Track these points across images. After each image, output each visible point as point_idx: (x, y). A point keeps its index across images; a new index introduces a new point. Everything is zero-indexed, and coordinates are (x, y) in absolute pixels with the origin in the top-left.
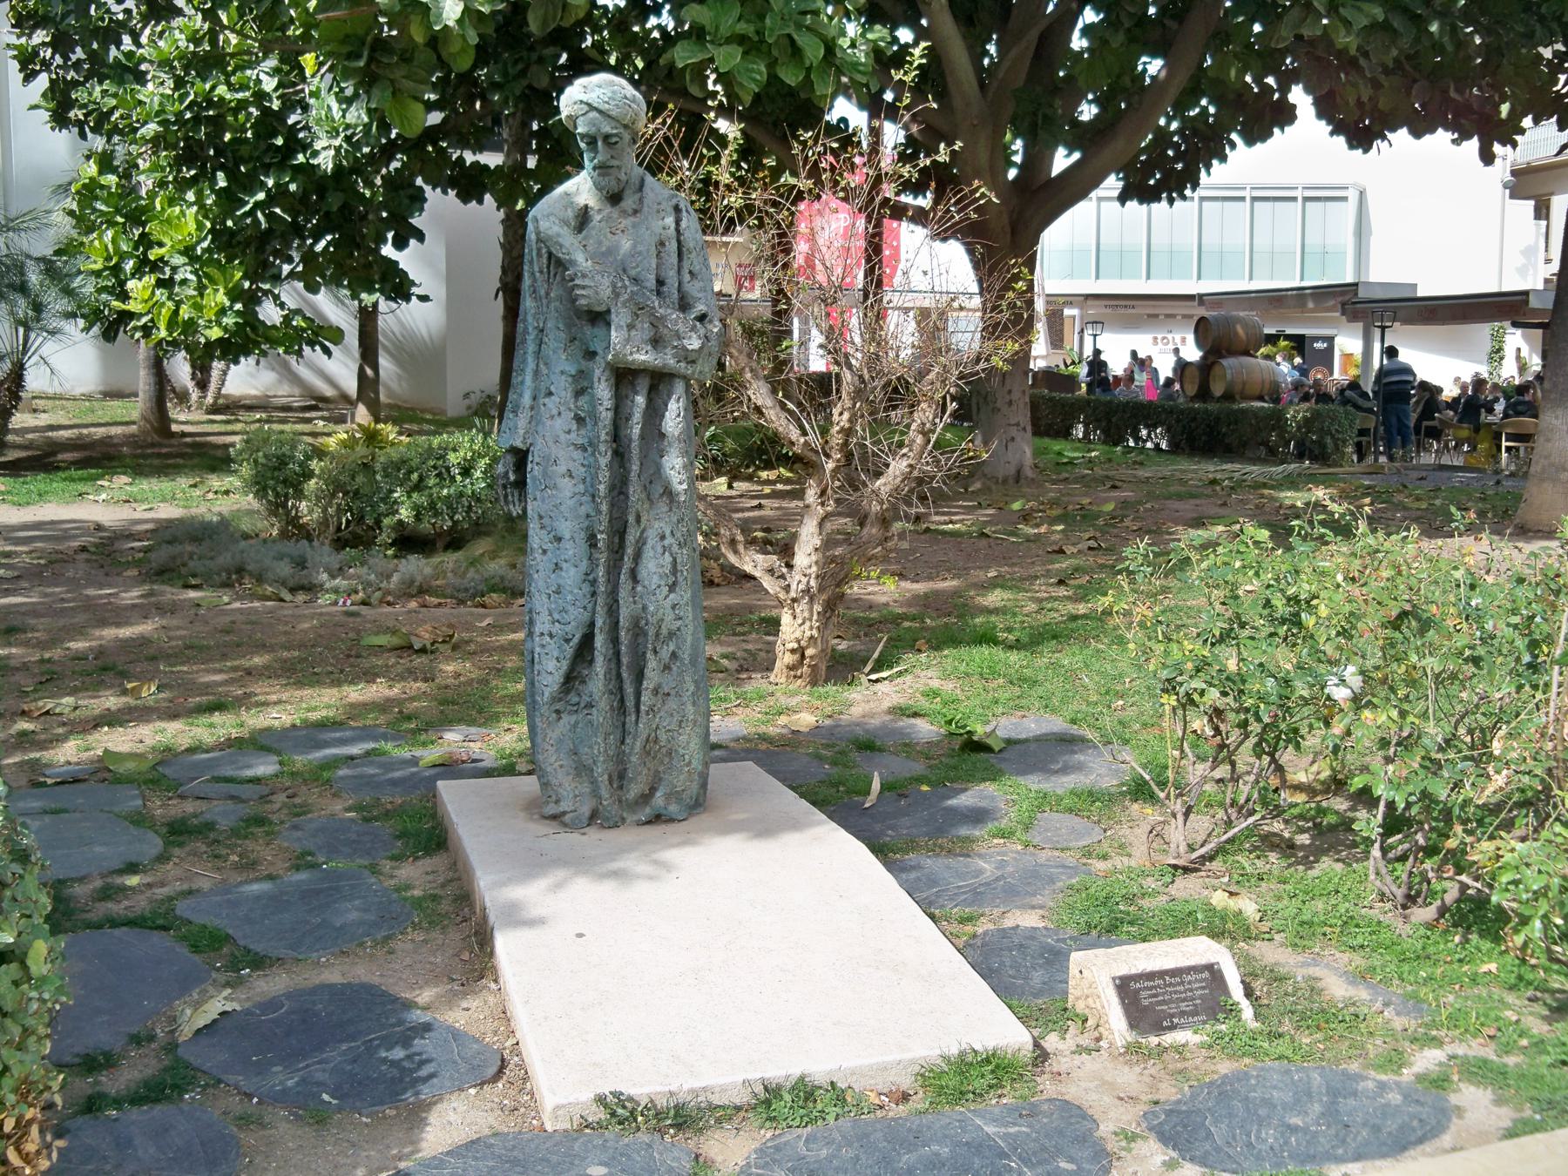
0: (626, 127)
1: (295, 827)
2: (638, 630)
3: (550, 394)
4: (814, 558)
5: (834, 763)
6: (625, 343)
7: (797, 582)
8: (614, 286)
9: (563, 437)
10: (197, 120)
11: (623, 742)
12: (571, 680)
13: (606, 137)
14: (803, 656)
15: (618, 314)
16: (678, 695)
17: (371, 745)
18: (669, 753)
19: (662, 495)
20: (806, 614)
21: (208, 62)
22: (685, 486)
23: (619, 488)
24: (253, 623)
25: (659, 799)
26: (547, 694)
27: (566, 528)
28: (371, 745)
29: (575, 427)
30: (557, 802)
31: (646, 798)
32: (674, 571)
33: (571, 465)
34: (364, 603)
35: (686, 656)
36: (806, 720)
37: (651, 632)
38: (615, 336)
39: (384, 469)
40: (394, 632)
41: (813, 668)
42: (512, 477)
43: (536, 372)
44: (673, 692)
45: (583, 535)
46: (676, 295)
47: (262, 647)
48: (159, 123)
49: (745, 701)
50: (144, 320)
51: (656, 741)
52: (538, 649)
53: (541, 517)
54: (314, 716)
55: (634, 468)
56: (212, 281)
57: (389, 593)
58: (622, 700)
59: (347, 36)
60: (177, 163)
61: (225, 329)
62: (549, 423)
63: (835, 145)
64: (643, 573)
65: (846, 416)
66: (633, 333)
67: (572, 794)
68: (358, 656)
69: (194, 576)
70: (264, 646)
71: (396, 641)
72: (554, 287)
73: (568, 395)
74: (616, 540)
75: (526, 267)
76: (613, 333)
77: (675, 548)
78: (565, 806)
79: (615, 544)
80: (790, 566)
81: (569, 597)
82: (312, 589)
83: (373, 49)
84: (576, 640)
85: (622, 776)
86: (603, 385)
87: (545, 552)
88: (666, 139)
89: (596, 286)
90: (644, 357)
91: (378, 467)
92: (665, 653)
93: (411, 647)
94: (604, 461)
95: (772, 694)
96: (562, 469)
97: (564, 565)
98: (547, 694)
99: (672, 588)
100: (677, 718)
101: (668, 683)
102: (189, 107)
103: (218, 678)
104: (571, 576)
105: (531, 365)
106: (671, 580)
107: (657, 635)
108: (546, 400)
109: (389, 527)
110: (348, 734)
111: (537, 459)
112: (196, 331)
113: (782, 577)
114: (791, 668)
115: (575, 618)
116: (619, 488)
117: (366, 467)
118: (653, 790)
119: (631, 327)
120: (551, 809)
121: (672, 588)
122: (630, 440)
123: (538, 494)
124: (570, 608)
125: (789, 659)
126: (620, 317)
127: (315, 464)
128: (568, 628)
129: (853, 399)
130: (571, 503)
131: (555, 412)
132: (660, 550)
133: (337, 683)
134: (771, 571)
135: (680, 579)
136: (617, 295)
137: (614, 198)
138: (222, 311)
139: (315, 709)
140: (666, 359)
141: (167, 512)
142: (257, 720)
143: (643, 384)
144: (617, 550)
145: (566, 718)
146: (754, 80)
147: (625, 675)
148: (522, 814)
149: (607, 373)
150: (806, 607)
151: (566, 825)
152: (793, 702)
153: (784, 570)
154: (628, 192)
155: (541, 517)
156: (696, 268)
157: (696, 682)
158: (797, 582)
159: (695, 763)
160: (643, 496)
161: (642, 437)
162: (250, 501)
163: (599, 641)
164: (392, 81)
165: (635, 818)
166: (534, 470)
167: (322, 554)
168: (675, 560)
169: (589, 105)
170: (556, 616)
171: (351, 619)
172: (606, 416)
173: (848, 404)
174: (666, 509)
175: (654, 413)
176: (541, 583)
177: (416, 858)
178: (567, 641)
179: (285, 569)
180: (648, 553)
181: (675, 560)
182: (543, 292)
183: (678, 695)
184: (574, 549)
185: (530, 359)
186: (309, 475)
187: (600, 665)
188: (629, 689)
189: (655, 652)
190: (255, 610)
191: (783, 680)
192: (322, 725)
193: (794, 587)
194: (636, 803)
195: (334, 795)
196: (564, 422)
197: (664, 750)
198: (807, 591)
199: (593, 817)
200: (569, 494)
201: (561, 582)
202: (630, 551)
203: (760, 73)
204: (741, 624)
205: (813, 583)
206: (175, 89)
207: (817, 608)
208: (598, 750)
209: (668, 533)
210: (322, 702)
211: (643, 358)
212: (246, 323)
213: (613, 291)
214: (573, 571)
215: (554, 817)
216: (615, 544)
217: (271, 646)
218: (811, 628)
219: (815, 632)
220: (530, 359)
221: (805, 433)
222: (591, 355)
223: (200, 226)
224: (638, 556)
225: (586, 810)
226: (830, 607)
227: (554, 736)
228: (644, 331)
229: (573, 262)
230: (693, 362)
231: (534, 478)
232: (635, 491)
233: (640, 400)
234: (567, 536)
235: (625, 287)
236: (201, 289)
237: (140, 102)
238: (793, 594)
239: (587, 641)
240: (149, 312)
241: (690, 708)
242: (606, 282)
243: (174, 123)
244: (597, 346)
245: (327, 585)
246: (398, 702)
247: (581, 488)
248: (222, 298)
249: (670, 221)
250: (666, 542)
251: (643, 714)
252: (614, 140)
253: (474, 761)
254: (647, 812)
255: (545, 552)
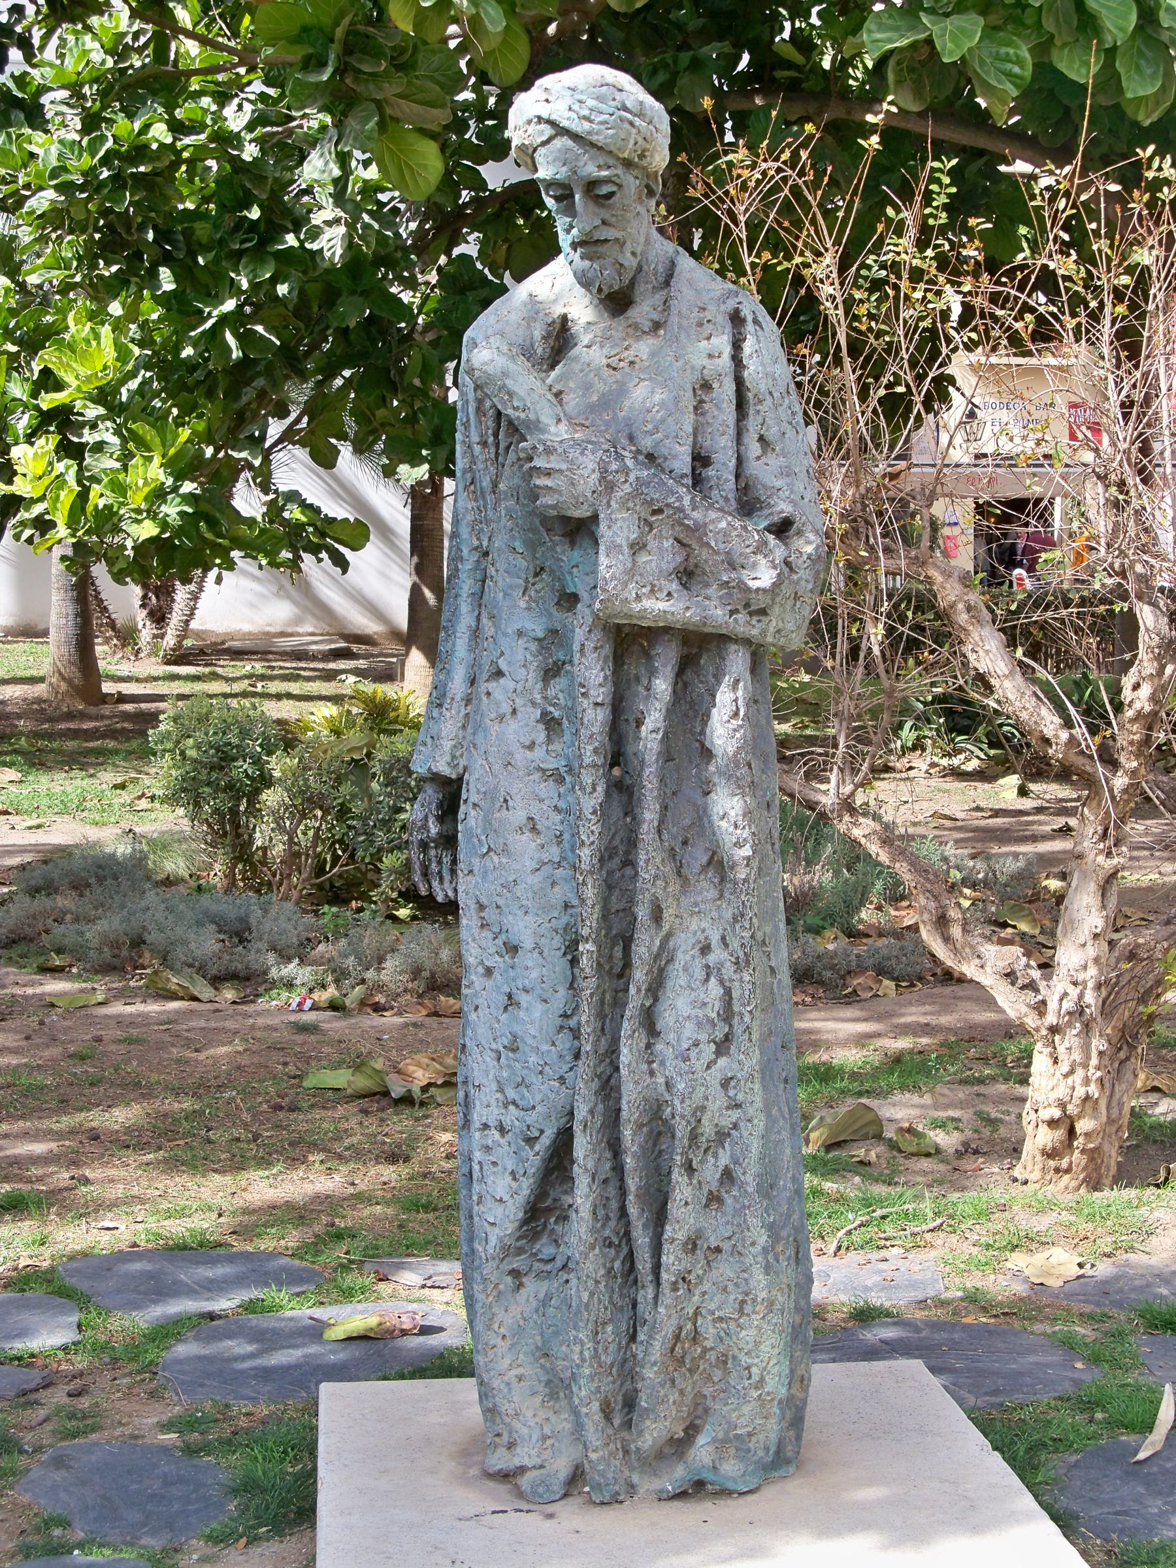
0: (628, 164)
1: (59, 1462)
2: (657, 1125)
3: (499, 674)
4: (1091, 952)
5: (1095, 1360)
6: (629, 577)
7: (1058, 993)
8: (604, 471)
9: (521, 757)
10: (118, 180)
11: (633, 1338)
12: (542, 1213)
13: (591, 186)
14: (1072, 1132)
15: (612, 522)
16: (736, 1252)
17: (255, 1293)
18: (723, 1361)
19: (705, 868)
20: (1077, 1056)
21: (125, 89)
22: (747, 851)
23: (619, 857)
24: (130, 1041)
25: (702, 1451)
26: (493, 1241)
27: (524, 929)
28: (255, 1293)
29: (541, 736)
30: (511, 1446)
31: (680, 1445)
32: (727, 1014)
33: (535, 810)
34: (334, 1006)
35: (750, 1179)
36: (1060, 1263)
37: (681, 1130)
38: (608, 565)
39: (386, 773)
40: (359, 1064)
41: (1093, 1155)
42: (434, 829)
43: (476, 633)
44: (726, 1246)
45: (557, 941)
46: (731, 485)
47: (134, 1088)
48: (57, 188)
49: (949, 1222)
50: (37, 509)
51: (696, 1337)
52: (478, 1155)
53: (481, 907)
54: (177, 1228)
55: (648, 815)
56: (142, 443)
57: (380, 987)
58: (631, 1257)
59: (305, 29)
60: (88, 259)
61: (164, 525)
62: (495, 728)
63: (1114, 188)
64: (666, 1020)
65: (1146, 690)
66: (643, 558)
67: (542, 1439)
68: (293, 1109)
69: (59, 951)
70: (138, 1085)
71: (362, 1082)
72: (507, 471)
73: (531, 676)
74: (618, 952)
75: (458, 436)
76: (603, 560)
77: (729, 971)
78: (525, 1455)
79: (613, 965)
80: (1046, 966)
81: (533, 1059)
82: (250, 982)
83: (348, 50)
84: (546, 1140)
85: (630, 1403)
86: (591, 657)
87: (489, 972)
88: (796, 191)
89: (572, 467)
90: (662, 605)
91: (377, 769)
92: (710, 1172)
93: (386, 1093)
94: (590, 803)
95: (1003, 1208)
96: (518, 816)
97: (523, 998)
98: (493, 1241)
99: (723, 1046)
100: (734, 1295)
101: (716, 1229)
102: (105, 161)
103: (39, 1148)
104: (536, 1019)
105: (466, 620)
106: (720, 1032)
107: (694, 1136)
108: (492, 686)
109: (392, 871)
110: (221, 1271)
111: (474, 798)
112: (117, 530)
113: (1031, 986)
114: (1050, 1154)
115: (544, 1094)
116: (619, 857)
117: (360, 767)
118: (692, 1430)
119: (637, 547)
120: (500, 1460)
121: (723, 1046)
122: (642, 763)
123: (476, 861)
124: (533, 1079)
125: (1045, 1137)
126: (617, 528)
127: (278, 765)
128: (531, 1118)
129: (1158, 658)
130: (535, 880)
131: (506, 708)
132: (699, 974)
133: (237, 1165)
134: (1010, 976)
135: (738, 1029)
136: (610, 487)
137: (616, 302)
138: (159, 494)
139: (182, 1213)
140: (710, 610)
141: (64, 832)
142: (72, 1237)
143: (666, 658)
144: (617, 972)
145: (532, 1286)
146: (1009, 75)
147: (633, 1210)
148: (450, 1465)
149: (597, 635)
150: (1076, 1042)
151: (521, 1495)
152: (1042, 1223)
153: (1036, 974)
154: (641, 288)
155: (481, 907)
156: (772, 433)
157: (771, 1228)
158: (1058, 993)
159: (771, 1384)
160: (668, 869)
161: (667, 756)
162: (172, 820)
163: (581, 1146)
164: (379, 105)
165: (656, 1484)
166: (470, 818)
167: (281, 916)
168: (728, 992)
169: (552, 123)
170: (511, 1094)
171: (299, 1038)
172: (596, 719)
173: (1149, 668)
174: (712, 894)
175: (689, 711)
176: (481, 1030)
177: (253, 1540)
178: (530, 1141)
179: (207, 944)
180: (677, 978)
181: (728, 992)
182: (486, 483)
183: (736, 1252)
184: (540, 968)
185: (465, 608)
186: (266, 781)
187: (583, 1195)
188: (642, 1239)
189: (690, 1169)
190: (144, 1020)
191: (1035, 1175)
192: (180, 1251)
193: (1052, 1005)
194: (660, 1455)
195: (152, 1395)
196: (522, 728)
197: (712, 1356)
198: (1079, 1011)
199: (576, 1477)
200: (530, 865)
201: (517, 1029)
202: (639, 975)
203: (1019, 62)
204: (984, 1060)
205: (1090, 998)
206: (85, 131)
207: (1098, 1044)
208: (579, 1351)
209: (715, 939)
210: (201, 1202)
211: (661, 605)
212: (198, 515)
213: (602, 479)
214: (538, 1009)
215: (505, 1476)
216: (613, 965)
217: (150, 1086)
218: (1087, 1081)
219: (1093, 1090)
220: (465, 608)
221: (1068, 724)
222: (569, 600)
223: (123, 355)
224: (656, 987)
225: (561, 1467)
226: (1125, 1042)
227: (508, 1320)
228: (662, 555)
229: (536, 426)
230: (763, 612)
231: (470, 833)
232: (650, 857)
233: (662, 686)
234: (528, 944)
235: (626, 471)
236: (126, 458)
237: (32, 156)
238: (1051, 1019)
239: (564, 1139)
240: (42, 499)
241: (759, 1279)
242: (589, 463)
243: (82, 187)
244: (578, 584)
245: (274, 973)
246: (327, 1203)
247: (554, 852)
248: (157, 473)
249: (722, 343)
250: (712, 959)
251: (666, 1288)
252: (605, 190)
253: (426, 1330)
254: (676, 1476)
255: (489, 972)
